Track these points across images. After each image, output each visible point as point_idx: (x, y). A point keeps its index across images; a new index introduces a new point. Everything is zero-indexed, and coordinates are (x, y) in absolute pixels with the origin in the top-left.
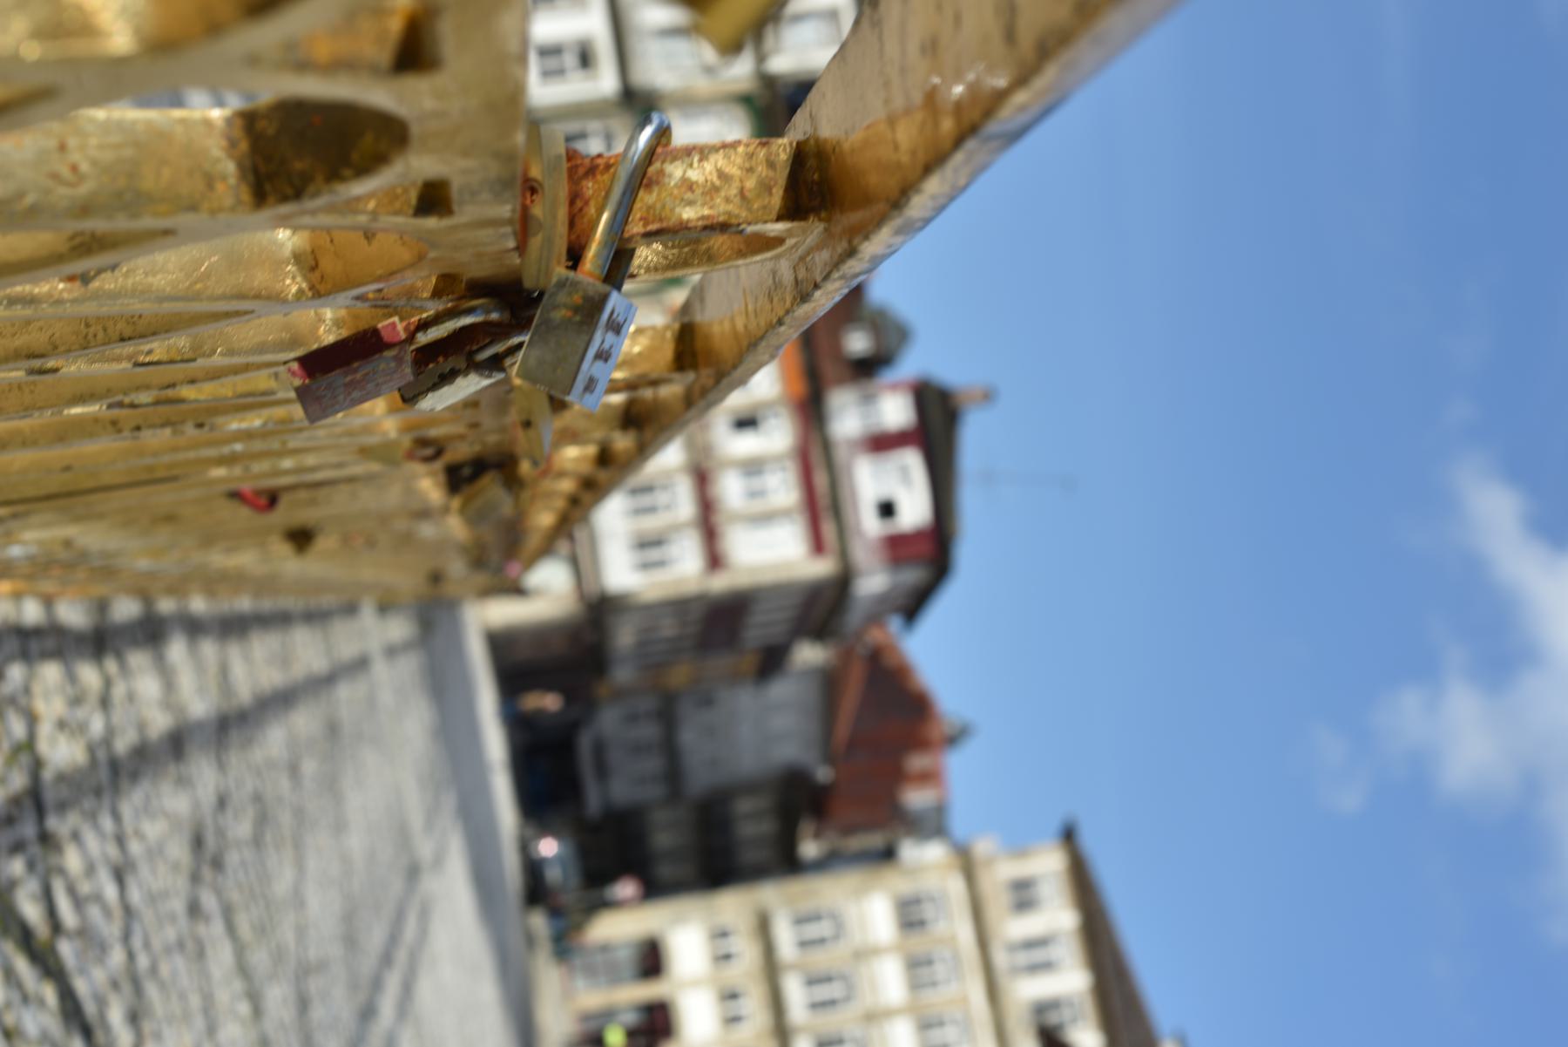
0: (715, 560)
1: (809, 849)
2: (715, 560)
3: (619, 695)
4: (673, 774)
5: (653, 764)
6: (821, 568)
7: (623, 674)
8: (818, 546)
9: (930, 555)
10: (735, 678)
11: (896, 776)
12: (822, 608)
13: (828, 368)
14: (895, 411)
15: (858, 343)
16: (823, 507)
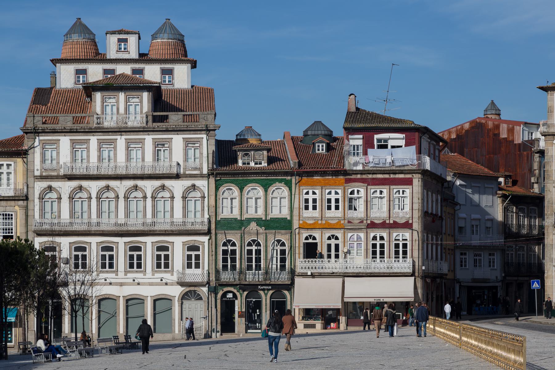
0: (407, 225)
1: (536, 189)
2: (407, 225)
3: (453, 270)
4: (491, 249)
5: (485, 258)
6: (417, 181)
7: (445, 268)
8: (409, 182)
9: (417, 134)
10: (453, 215)
11: (509, 142)
12: (433, 182)
13: (334, 166)
14: (357, 140)
15: (321, 149)
16: (392, 177)
